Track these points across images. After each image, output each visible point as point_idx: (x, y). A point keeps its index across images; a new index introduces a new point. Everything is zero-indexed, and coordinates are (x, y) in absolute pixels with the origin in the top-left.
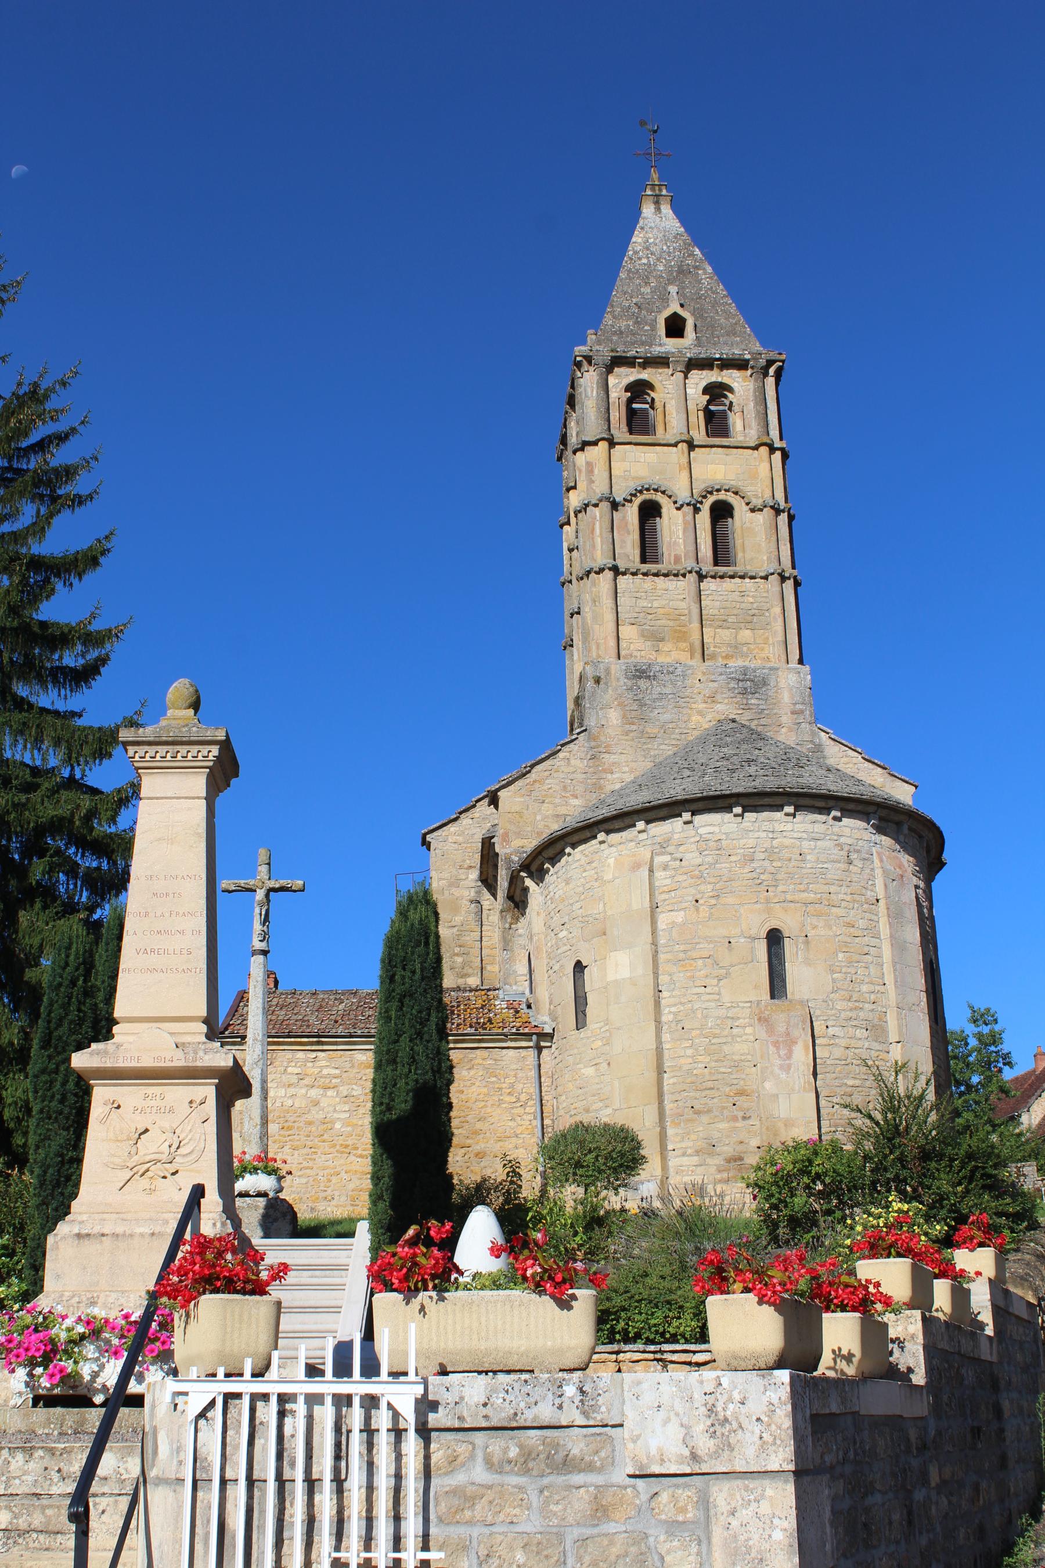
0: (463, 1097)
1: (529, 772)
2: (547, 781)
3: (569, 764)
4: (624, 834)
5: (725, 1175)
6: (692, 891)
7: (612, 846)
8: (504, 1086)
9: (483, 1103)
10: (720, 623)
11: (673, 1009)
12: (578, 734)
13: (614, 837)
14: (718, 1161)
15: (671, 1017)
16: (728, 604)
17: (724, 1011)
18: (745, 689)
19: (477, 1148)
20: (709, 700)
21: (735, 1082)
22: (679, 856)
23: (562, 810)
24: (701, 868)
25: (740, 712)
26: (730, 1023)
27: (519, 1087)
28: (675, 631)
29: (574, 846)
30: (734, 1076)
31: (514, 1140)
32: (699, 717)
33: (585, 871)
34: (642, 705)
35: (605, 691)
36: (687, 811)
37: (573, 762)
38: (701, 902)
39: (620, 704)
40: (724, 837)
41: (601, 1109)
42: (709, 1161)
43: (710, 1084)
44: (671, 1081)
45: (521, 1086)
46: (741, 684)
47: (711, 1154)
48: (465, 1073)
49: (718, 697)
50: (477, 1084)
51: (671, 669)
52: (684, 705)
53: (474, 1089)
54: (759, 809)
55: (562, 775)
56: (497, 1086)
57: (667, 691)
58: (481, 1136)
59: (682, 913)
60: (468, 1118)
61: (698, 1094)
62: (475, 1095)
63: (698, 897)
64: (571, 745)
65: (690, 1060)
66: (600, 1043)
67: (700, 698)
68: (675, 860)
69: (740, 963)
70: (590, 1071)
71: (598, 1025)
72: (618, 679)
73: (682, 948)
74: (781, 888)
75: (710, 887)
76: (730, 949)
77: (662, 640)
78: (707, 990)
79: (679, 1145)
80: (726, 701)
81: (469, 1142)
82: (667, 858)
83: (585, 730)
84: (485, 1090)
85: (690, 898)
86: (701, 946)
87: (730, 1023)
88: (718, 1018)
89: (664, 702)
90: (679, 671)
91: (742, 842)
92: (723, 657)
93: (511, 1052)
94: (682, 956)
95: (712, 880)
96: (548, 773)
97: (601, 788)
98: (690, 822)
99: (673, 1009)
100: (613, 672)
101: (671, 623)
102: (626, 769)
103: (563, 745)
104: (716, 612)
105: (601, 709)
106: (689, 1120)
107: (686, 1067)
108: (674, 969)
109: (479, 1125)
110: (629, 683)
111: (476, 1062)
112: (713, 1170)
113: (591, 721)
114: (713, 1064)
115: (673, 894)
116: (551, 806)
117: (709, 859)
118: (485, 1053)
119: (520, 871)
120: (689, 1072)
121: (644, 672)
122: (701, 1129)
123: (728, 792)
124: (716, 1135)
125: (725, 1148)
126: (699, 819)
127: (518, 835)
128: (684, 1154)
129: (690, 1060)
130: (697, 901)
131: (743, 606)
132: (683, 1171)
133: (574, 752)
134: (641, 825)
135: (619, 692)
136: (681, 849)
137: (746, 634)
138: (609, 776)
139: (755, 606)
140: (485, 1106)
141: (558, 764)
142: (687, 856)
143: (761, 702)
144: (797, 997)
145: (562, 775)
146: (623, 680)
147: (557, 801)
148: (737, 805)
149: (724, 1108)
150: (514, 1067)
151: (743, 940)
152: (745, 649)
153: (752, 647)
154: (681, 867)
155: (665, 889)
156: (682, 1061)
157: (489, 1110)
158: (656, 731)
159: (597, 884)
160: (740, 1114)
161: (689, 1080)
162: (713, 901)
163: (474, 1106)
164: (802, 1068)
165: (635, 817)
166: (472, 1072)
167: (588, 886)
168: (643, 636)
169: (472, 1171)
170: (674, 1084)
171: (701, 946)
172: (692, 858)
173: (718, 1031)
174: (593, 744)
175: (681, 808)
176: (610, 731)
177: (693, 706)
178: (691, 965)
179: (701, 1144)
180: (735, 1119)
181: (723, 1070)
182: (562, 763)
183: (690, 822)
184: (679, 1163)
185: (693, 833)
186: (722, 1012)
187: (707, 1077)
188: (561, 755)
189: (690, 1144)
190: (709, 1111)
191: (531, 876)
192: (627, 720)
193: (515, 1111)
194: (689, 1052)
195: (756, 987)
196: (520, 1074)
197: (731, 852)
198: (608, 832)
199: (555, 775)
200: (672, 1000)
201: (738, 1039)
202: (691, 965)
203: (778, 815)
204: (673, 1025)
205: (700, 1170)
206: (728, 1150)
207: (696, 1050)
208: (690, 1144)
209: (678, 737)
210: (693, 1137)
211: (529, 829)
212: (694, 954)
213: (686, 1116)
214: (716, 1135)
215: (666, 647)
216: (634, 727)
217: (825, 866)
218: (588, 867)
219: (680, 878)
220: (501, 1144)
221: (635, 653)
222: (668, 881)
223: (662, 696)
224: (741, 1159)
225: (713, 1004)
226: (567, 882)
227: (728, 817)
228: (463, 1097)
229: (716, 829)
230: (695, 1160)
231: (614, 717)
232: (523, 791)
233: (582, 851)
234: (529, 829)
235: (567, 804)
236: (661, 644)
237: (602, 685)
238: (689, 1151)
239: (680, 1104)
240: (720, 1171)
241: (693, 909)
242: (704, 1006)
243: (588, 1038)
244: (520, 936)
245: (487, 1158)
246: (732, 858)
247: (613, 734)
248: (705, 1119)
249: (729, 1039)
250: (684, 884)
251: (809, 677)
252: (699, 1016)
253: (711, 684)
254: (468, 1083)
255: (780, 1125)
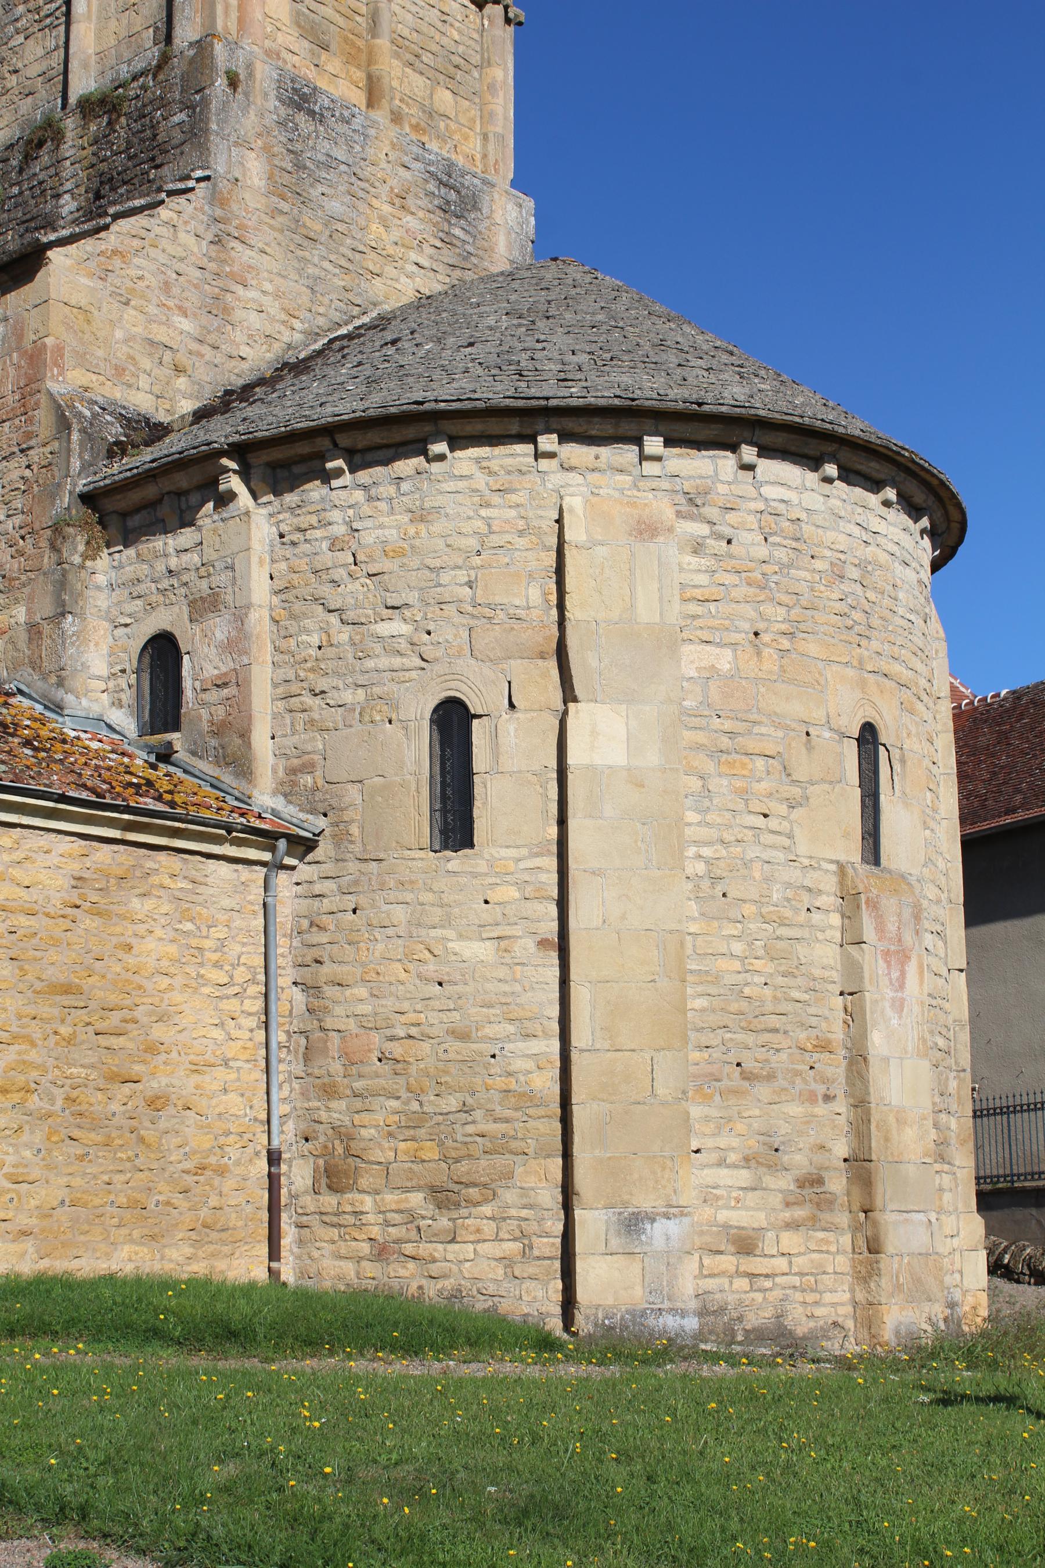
0: (131, 960)
1: (106, 227)
2: (136, 261)
3: (175, 239)
4: (606, 453)
5: (800, 1213)
6: (748, 610)
7: (571, 469)
8: (208, 944)
9: (164, 982)
10: (412, 58)
11: (706, 852)
12: (199, 180)
13: (574, 452)
14: (785, 1182)
15: (701, 868)
16: (424, 27)
17: (798, 873)
18: (448, 203)
19: (154, 1085)
20: (397, 201)
21: (814, 1021)
22: (727, 531)
23: (161, 334)
24: (768, 569)
25: (439, 244)
26: (806, 900)
27: (234, 949)
28: (346, 40)
29: (456, 443)
30: (812, 1010)
31: (220, 1072)
32: (382, 229)
33: (488, 505)
34: (300, 166)
35: (245, 110)
36: (751, 443)
37: (182, 235)
38: (765, 638)
39: (266, 149)
40: (803, 516)
41: (508, 1038)
42: (769, 1181)
43: (774, 1021)
44: (700, 1003)
45: (238, 948)
46: (443, 190)
47: (774, 1168)
48: (136, 903)
49: (410, 202)
50: (159, 932)
51: (346, 113)
52: (361, 194)
53: (150, 944)
54: (852, 476)
55: (163, 258)
56: (194, 942)
57: (340, 154)
58: (163, 1057)
59: (728, 653)
60: (138, 1013)
61: (750, 1039)
62: (151, 963)
63: (760, 626)
64: (181, 200)
65: (737, 965)
66: (514, 893)
67: (384, 190)
68: (719, 536)
69: (823, 780)
70: (478, 950)
71: (512, 853)
72: (266, 94)
73: (728, 725)
74: (875, 645)
75: (782, 611)
76: (809, 747)
77: (325, 48)
78: (773, 823)
79: (710, 1143)
80: (421, 214)
81: (138, 1068)
82: (704, 529)
83: (208, 178)
84: (173, 949)
85: (746, 626)
86: (763, 730)
87: (806, 900)
88: (788, 885)
89: (332, 176)
90: (357, 122)
91: (830, 536)
92: (411, 126)
93: (224, 868)
94: (725, 742)
95: (785, 598)
96: (136, 243)
97: (227, 310)
98: (750, 468)
99: (706, 852)
100: (258, 76)
101: (341, 21)
102: (268, 287)
103: (171, 193)
104: (406, 33)
105: (236, 144)
106: (735, 1092)
107: (729, 979)
108: (710, 767)
109: (158, 1032)
110: (283, 111)
111: (155, 879)
112: (777, 1200)
113: (219, 166)
114: (780, 980)
115: (712, 606)
116: (141, 317)
117: (781, 554)
118: (173, 862)
119: (221, 453)
120: (737, 991)
121: (305, 98)
122: (757, 1112)
123: (841, 430)
124: (784, 1129)
125: (798, 1157)
126: (771, 468)
127: (82, 360)
128: (721, 1163)
129: (737, 965)
130: (756, 634)
131: (445, 41)
132: (718, 1198)
133: (185, 216)
134: (654, 444)
135: (267, 122)
136: (731, 517)
137: (444, 98)
138: (240, 290)
139: (461, 49)
140: (171, 988)
141: (158, 230)
142: (744, 537)
143: (467, 238)
144: (893, 866)
145: (163, 258)
146: (273, 103)
147: (152, 309)
148: (833, 459)
149: (798, 1073)
150: (227, 903)
151: (827, 734)
152: (442, 125)
153: (453, 126)
154: (731, 556)
155: (698, 593)
156: (723, 964)
157: (177, 997)
158: (318, 227)
159: (521, 542)
160: (821, 1089)
161: (734, 1007)
162: (785, 644)
163: (148, 985)
164: (916, 1009)
165: (649, 424)
166: (149, 904)
167: (495, 540)
168: (299, 26)
169: (142, 1140)
170: (703, 1010)
171: (763, 730)
172: (750, 543)
173: (788, 913)
174: (218, 212)
175: (747, 434)
176: (247, 196)
177: (375, 202)
178: (744, 766)
179: (753, 1144)
180: (812, 1098)
181: (796, 994)
182: (163, 231)
183: (750, 468)
184: (710, 1181)
185: (753, 493)
186: (793, 875)
187: (769, 1007)
188: (163, 213)
189: (735, 1142)
190: (771, 1077)
191: (245, 475)
192: (276, 189)
193: (225, 1005)
194: (738, 947)
195: (846, 835)
196: (238, 923)
197: (816, 551)
198: (565, 437)
199: (153, 252)
200: (704, 833)
201: (820, 936)
202: (744, 766)
203: (873, 500)
204: (706, 884)
205: (751, 1198)
206: (799, 1160)
207: (750, 944)
208: (735, 1142)
209: (350, 254)
210: (740, 1127)
211: (100, 353)
212: (752, 745)
213: (725, 1083)
214: (784, 1129)
215: (333, 64)
216: (285, 206)
217: (912, 617)
218: (496, 499)
219: (729, 579)
220: (196, 1078)
221: (284, 54)
222: (703, 579)
223: (330, 163)
224: (820, 1181)
225: (780, 856)
226: (420, 516)
227: (812, 478)
228: (131, 960)
229: (791, 496)
230: (744, 1177)
231: (255, 170)
232: (92, 264)
233: (478, 461)
234: (100, 353)
235: (168, 323)
236: (324, 56)
237: (240, 96)
238: (732, 1157)
239: (716, 1054)
240: (788, 1205)
241: (750, 650)
242: (765, 856)
243: (475, 875)
244: (98, 588)
245: (171, 1110)
246: (818, 564)
247: (252, 205)
248: (763, 1091)
249: (805, 933)
250: (735, 593)
251: (532, 219)
252: (757, 875)
253: (402, 171)
254: (141, 929)
255: (891, 1119)
